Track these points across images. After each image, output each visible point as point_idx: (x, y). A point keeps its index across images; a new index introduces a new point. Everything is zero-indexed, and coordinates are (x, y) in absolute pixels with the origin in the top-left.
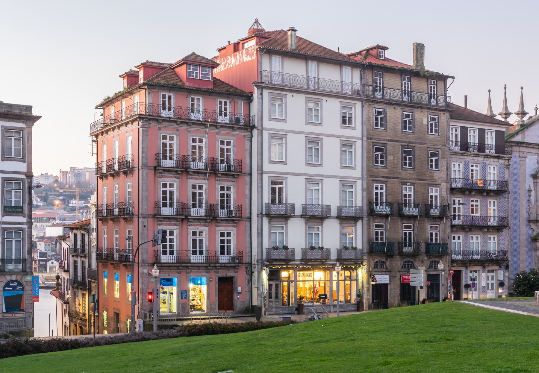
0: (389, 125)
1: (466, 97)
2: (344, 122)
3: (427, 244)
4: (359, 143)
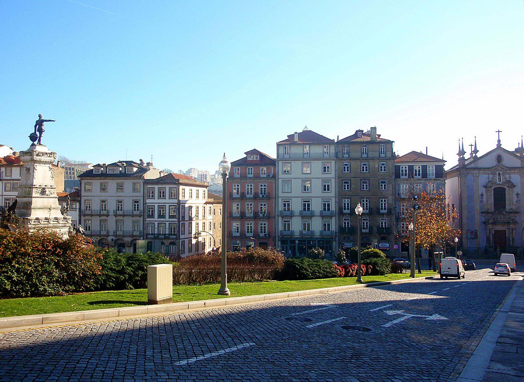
2: (325, 171)
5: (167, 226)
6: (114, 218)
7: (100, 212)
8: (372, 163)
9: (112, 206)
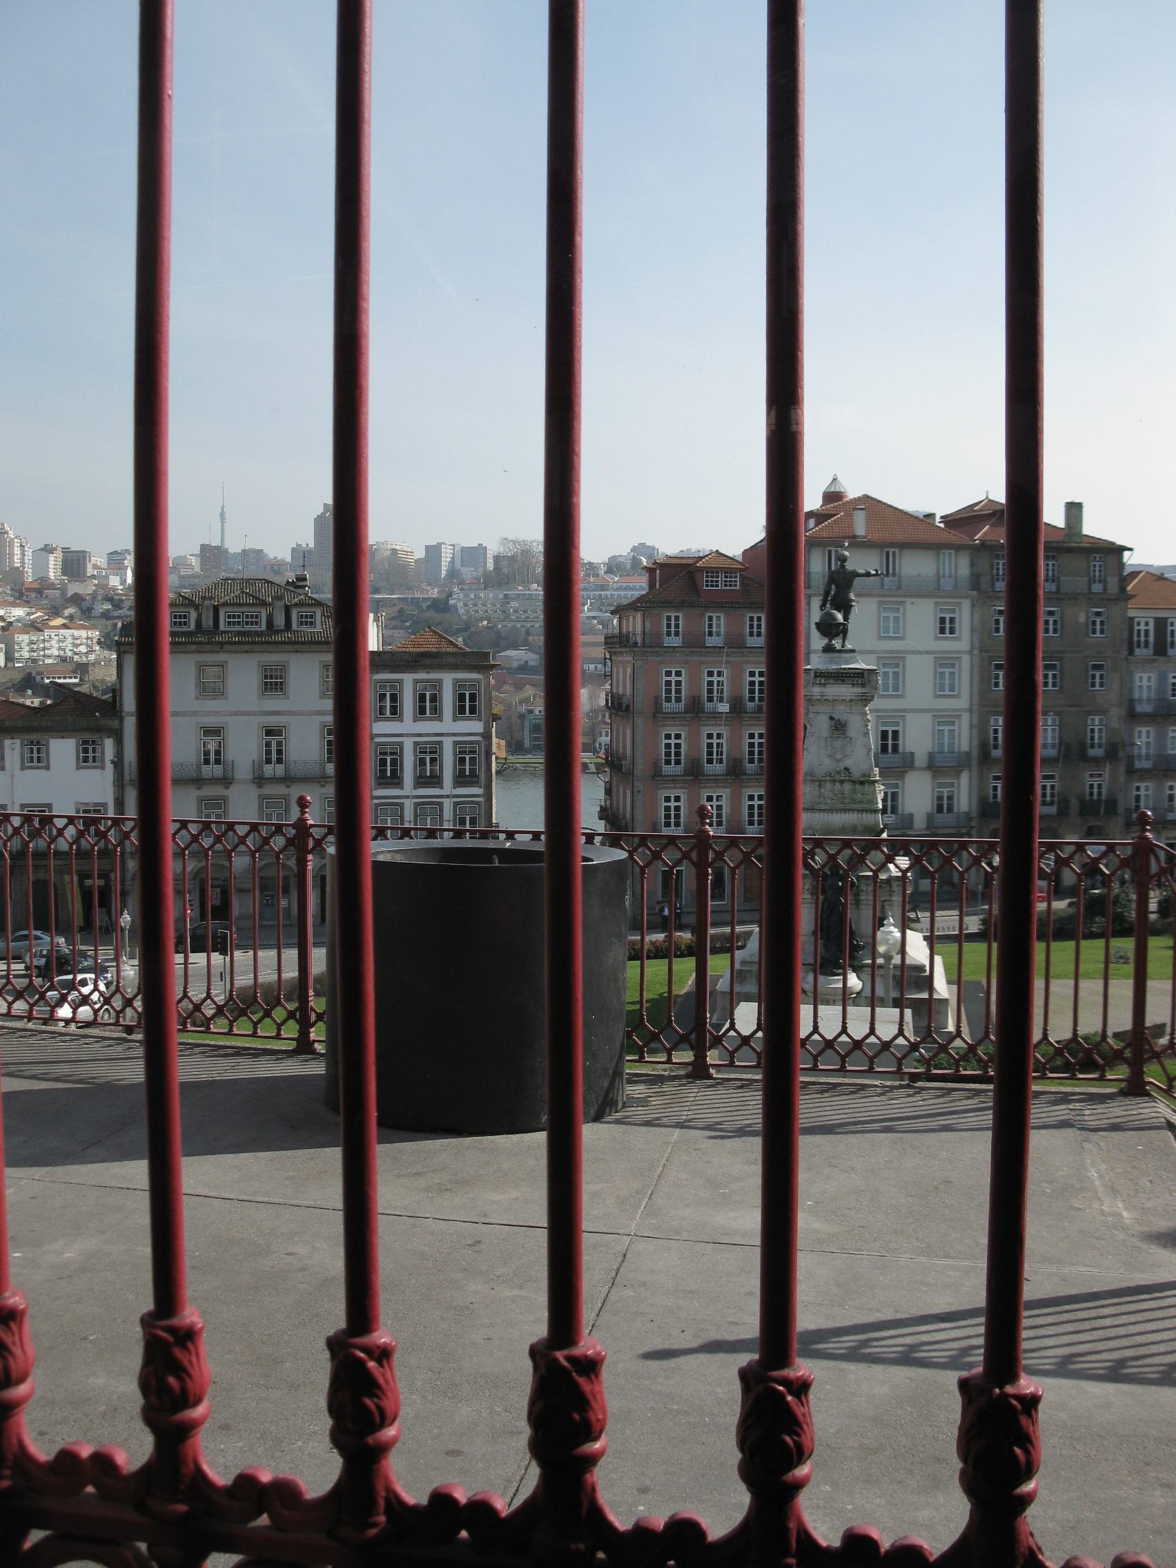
2: (942, 631)
3: (1082, 802)
4: (966, 659)
5: (448, 813)
6: (253, 793)
7: (200, 770)
9: (244, 749)
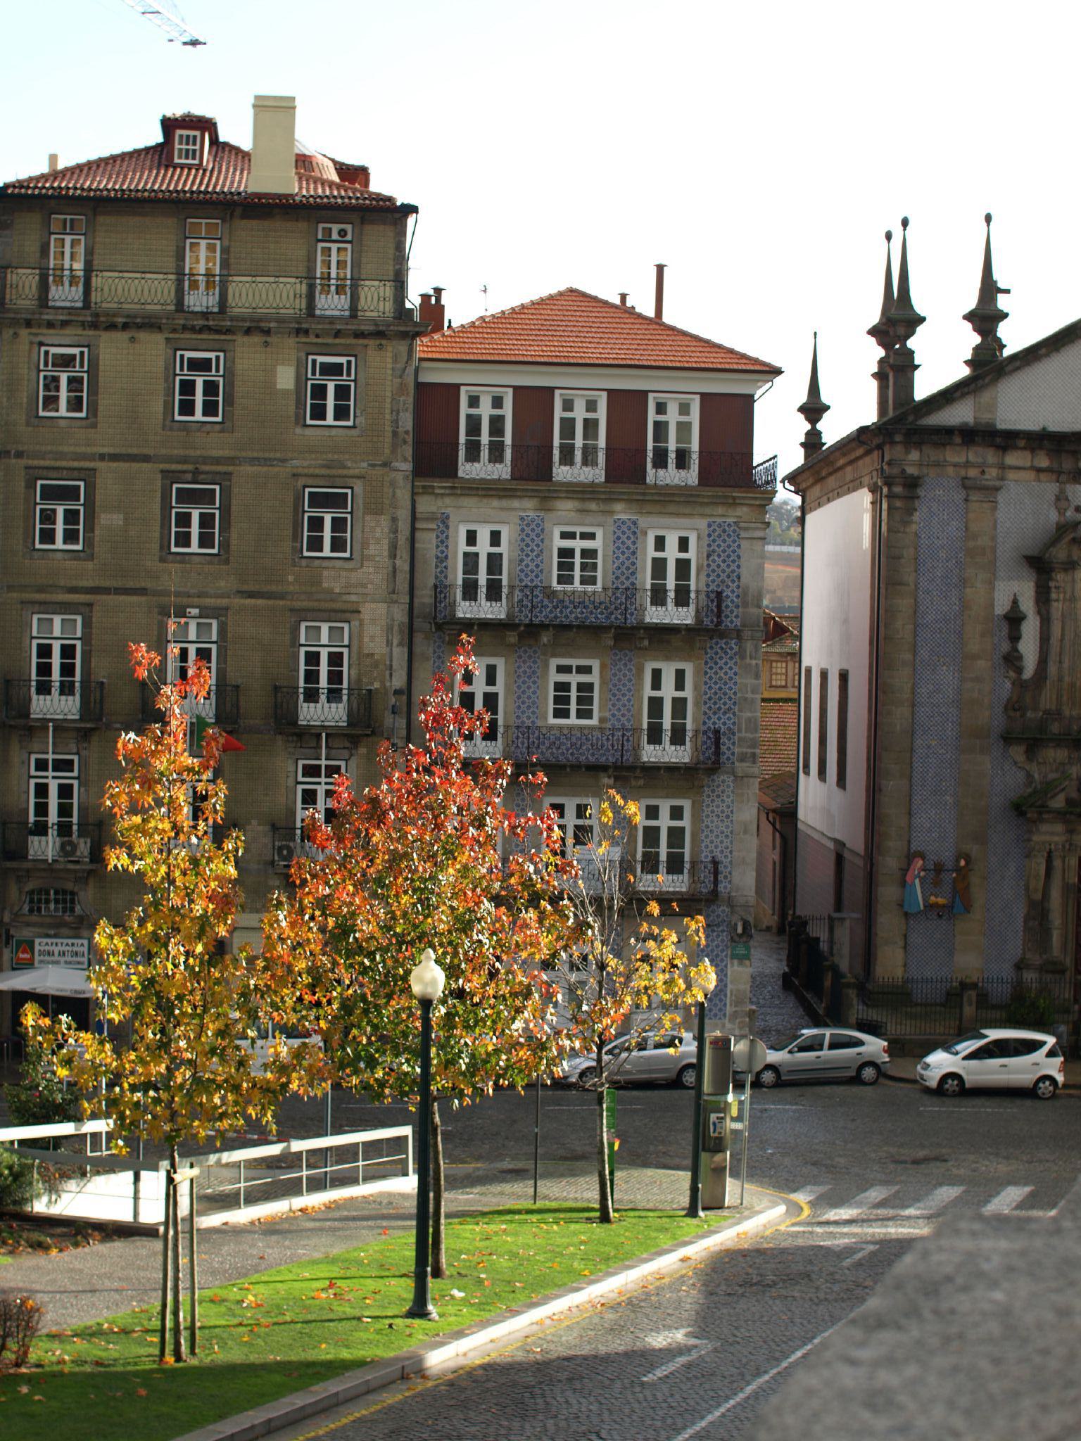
0: (104, 402)
1: (660, 269)
8: (248, 355)
